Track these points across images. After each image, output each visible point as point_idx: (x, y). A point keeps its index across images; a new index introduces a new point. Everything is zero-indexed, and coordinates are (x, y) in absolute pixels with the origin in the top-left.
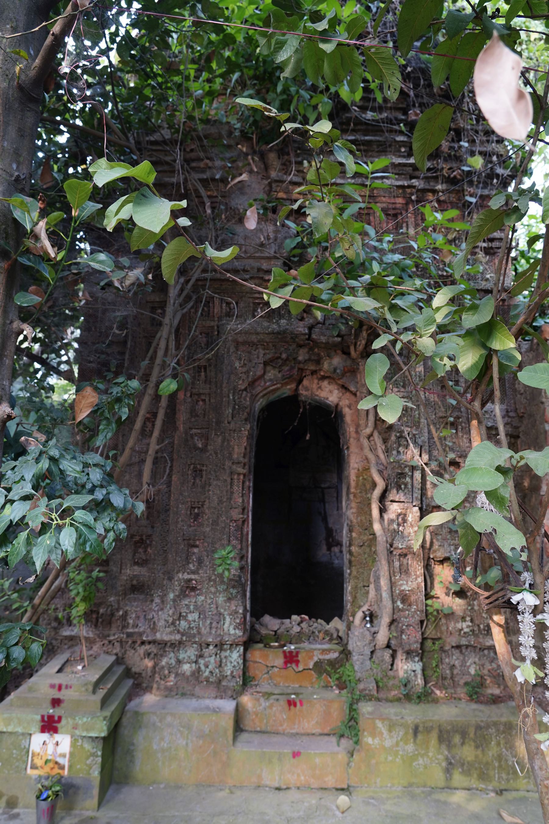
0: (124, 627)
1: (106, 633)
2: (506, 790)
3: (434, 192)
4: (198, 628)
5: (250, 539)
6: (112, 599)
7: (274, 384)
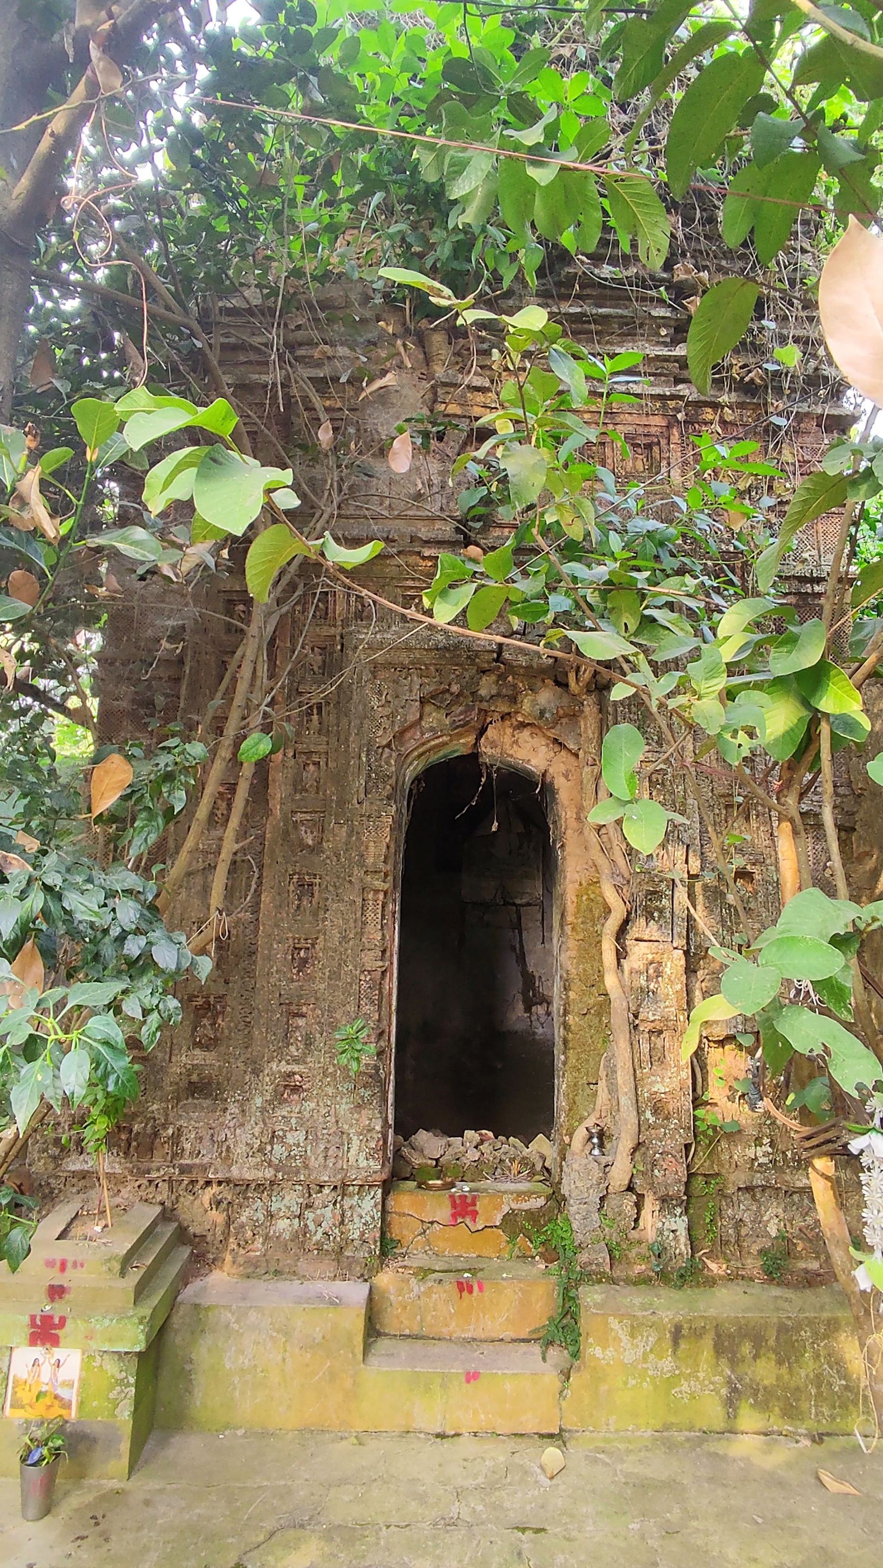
0: (175, 1155)
1: (144, 1166)
2: (828, 1434)
3: (715, 406)
4: (304, 1157)
5: (394, 1003)
6: (155, 1107)
7: (437, 737)
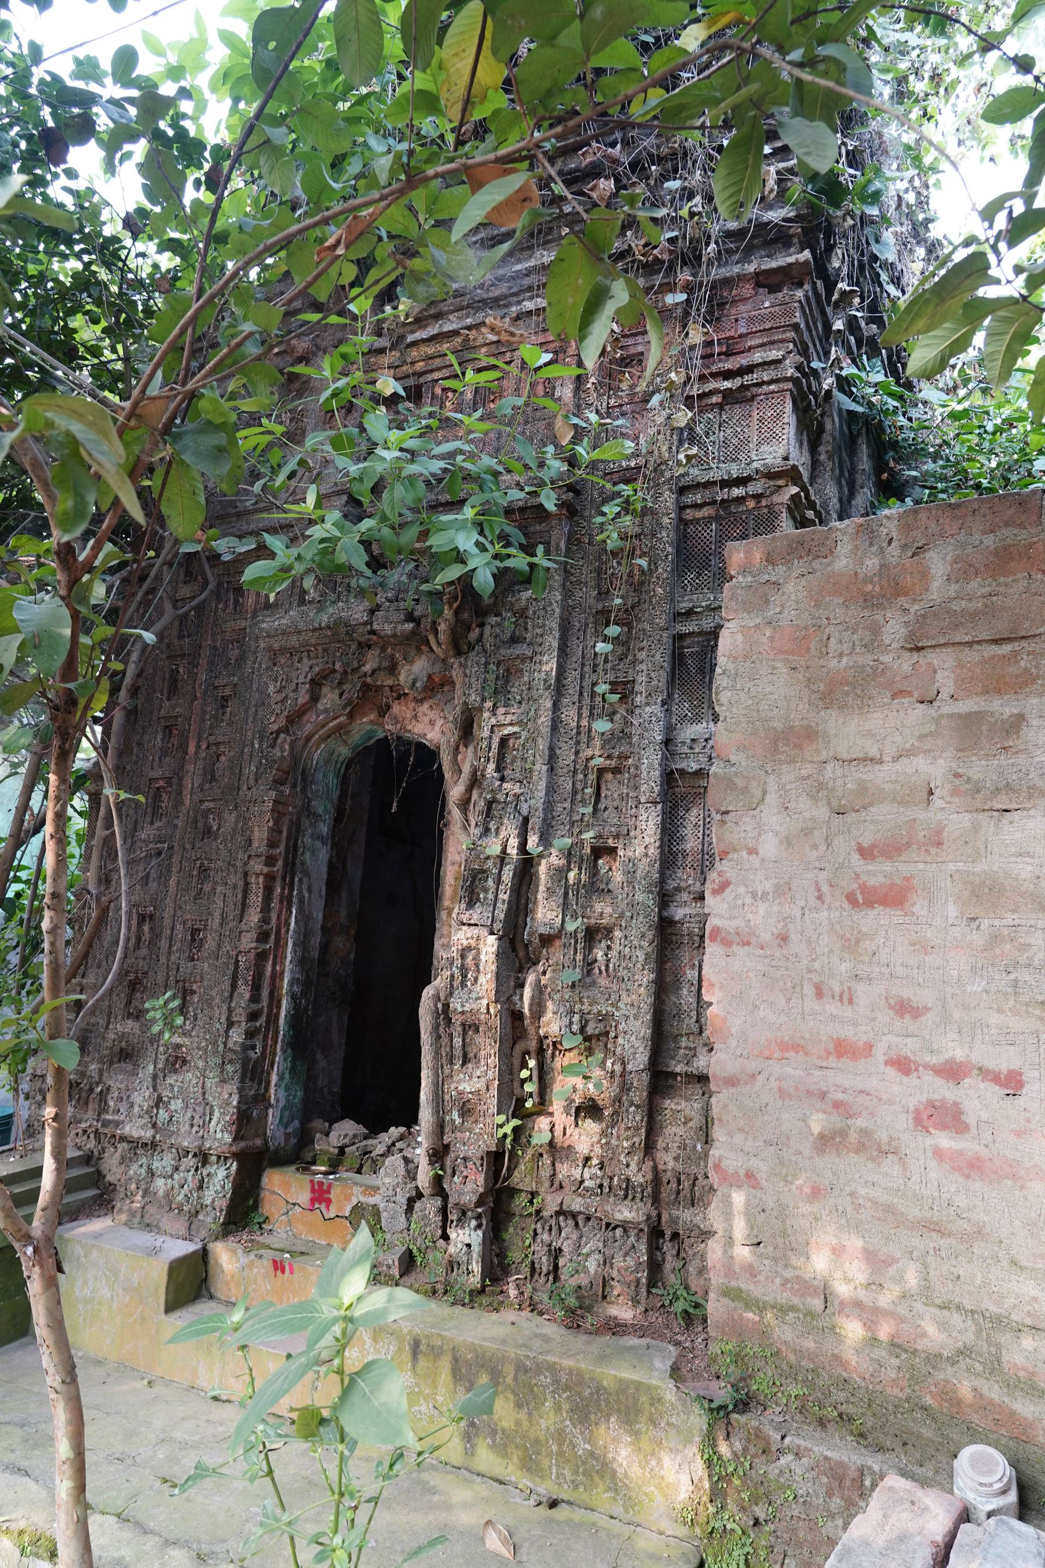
2: (569, 1503)
